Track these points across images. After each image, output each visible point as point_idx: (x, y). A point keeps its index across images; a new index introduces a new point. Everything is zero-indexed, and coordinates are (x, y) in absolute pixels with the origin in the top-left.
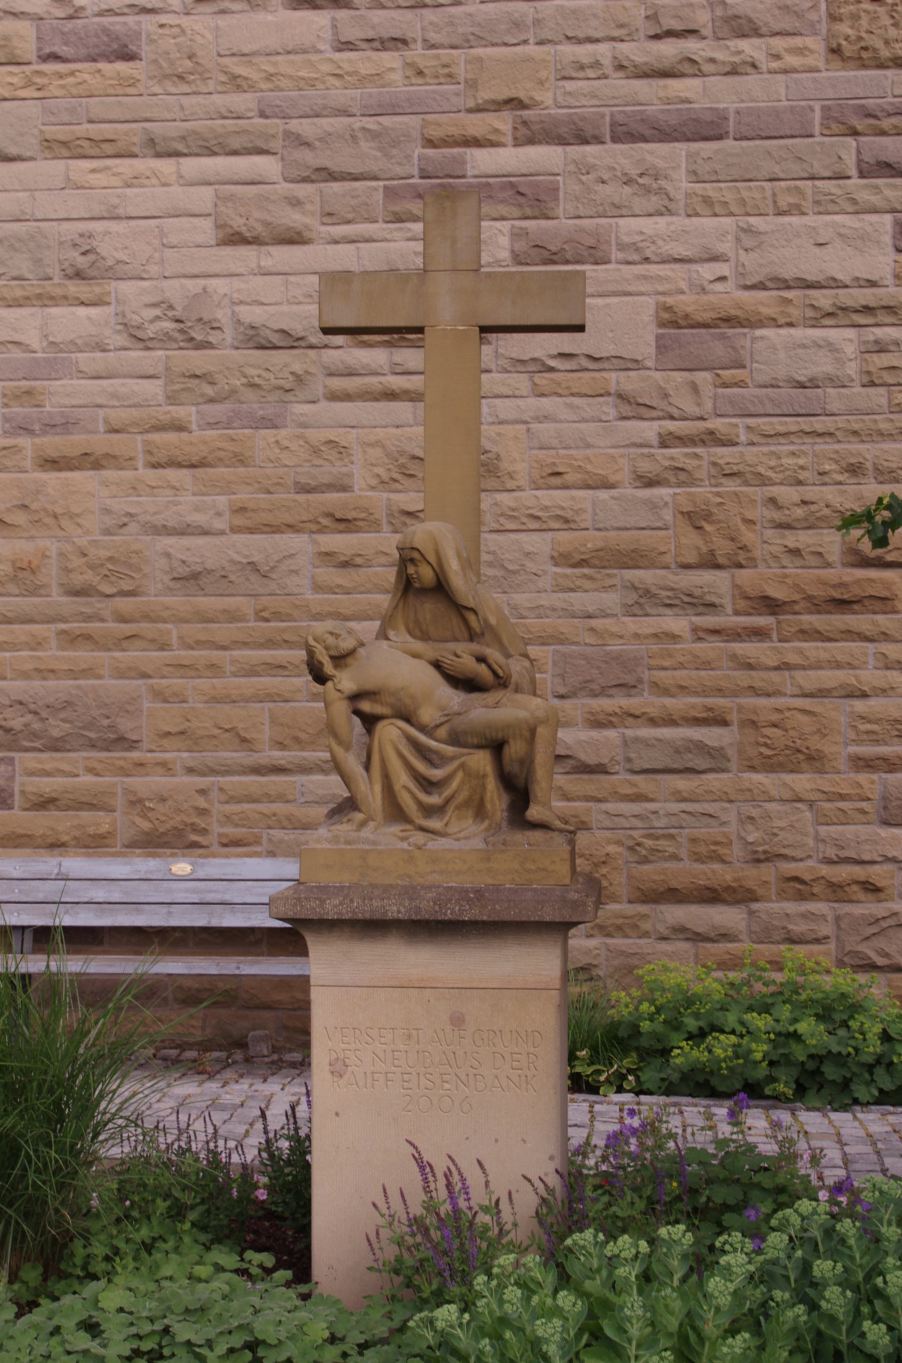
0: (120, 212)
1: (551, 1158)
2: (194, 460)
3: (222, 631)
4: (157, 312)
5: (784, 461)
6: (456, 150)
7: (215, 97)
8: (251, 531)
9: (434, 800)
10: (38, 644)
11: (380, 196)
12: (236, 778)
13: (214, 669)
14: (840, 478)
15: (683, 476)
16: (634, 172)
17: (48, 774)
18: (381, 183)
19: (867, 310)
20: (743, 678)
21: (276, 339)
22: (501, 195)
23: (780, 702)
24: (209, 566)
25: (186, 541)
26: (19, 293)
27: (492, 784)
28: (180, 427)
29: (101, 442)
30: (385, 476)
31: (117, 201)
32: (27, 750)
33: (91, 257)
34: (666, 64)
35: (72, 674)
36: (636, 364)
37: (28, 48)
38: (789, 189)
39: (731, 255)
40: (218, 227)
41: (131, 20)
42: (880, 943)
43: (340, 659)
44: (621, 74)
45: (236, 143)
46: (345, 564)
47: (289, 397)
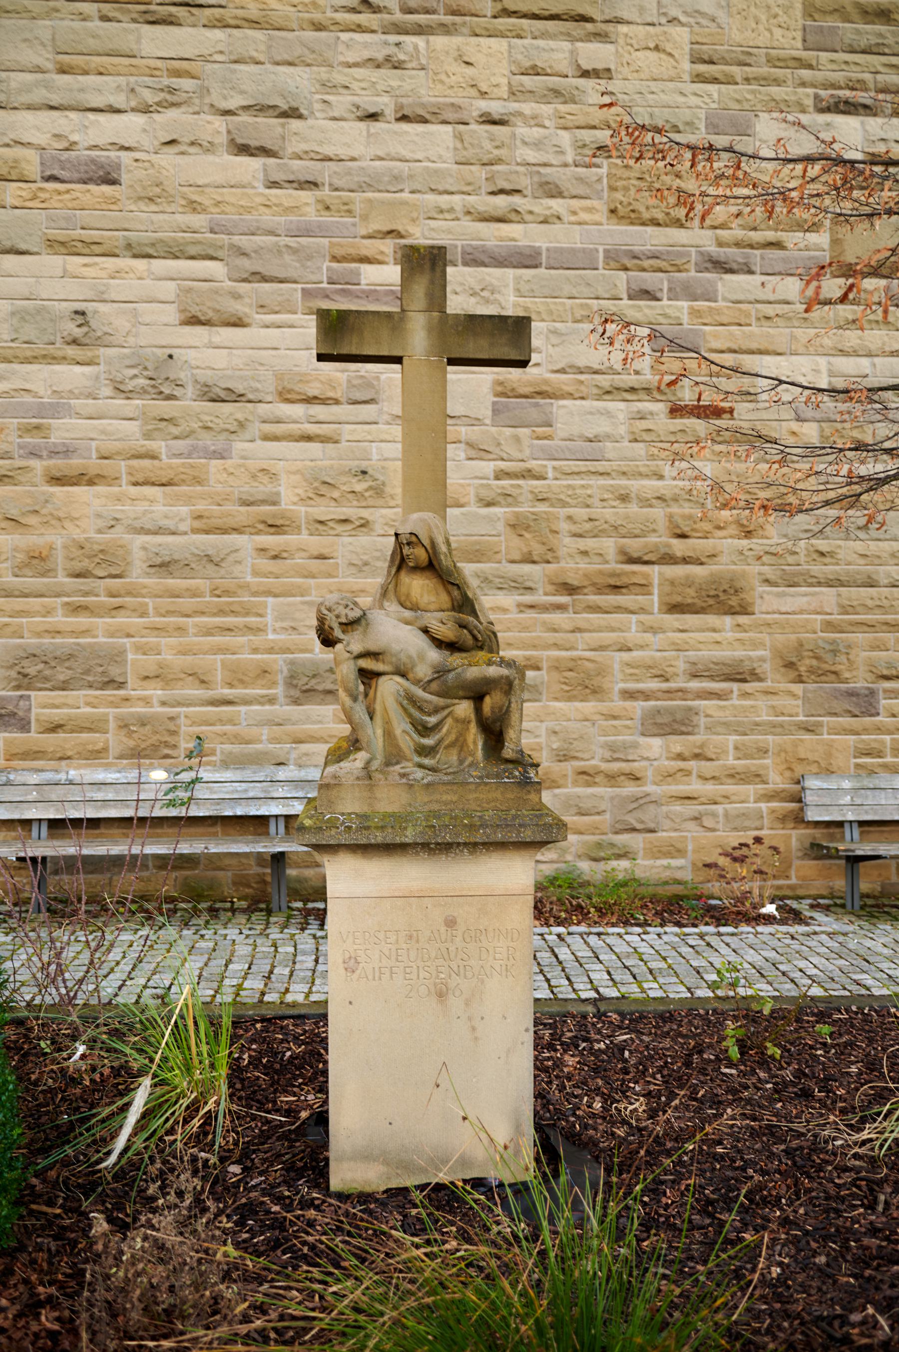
0: (105, 296)
1: (527, 1030)
2: (164, 481)
3: (187, 603)
4: (135, 371)
5: (578, 491)
6: (354, 265)
7: (178, 217)
8: (207, 532)
9: (429, 742)
10: (48, 613)
11: (299, 294)
12: (197, 709)
13: (181, 630)
14: (615, 503)
15: (510, 499)
16: (477, 288)
17: (57, 707)
18: (300, 286)
19: (633, 390)
20: (550, 637)
21: (223, 394)
22: (385, 299)
23: (574, 653)
24: (176, 557)
25: (159, 539)
26: (29, 354)
27: (473, 728)
28: (153, 456)
29: (93, 464)
30: (303, 495)
31: (103, 288)
32: (40, 689)
33: (85, 329)
34: (499, 213)
35: (73, 633)
36: (478, 421)
37: (33, 169)
38: (582, 305)
39: (544, 348)
40: (182, 311)
41: (113, 154)
42: (638, 814)
43: (349, 625)
44: (468, 218)
45: (192, 250)
46: (275, 557)
47: (233, 437)
